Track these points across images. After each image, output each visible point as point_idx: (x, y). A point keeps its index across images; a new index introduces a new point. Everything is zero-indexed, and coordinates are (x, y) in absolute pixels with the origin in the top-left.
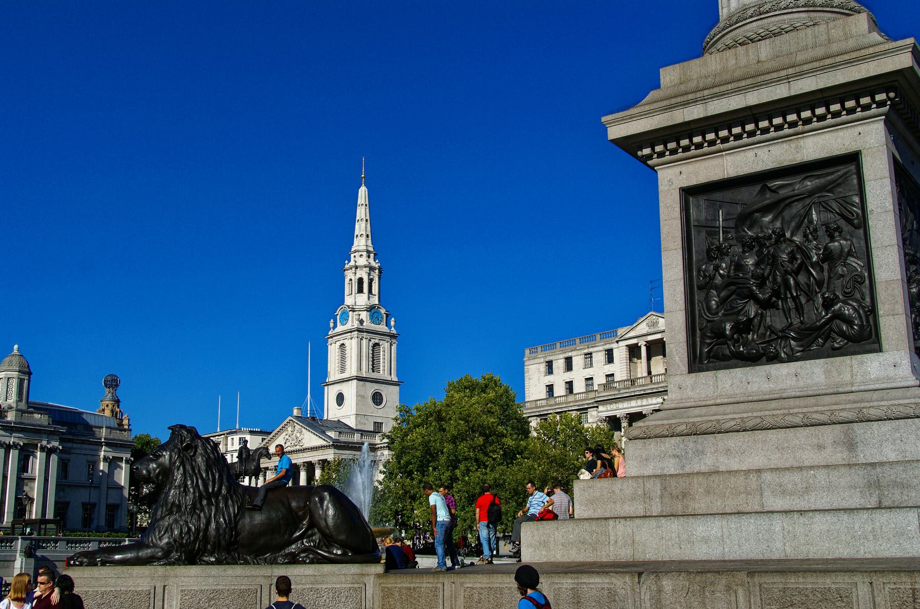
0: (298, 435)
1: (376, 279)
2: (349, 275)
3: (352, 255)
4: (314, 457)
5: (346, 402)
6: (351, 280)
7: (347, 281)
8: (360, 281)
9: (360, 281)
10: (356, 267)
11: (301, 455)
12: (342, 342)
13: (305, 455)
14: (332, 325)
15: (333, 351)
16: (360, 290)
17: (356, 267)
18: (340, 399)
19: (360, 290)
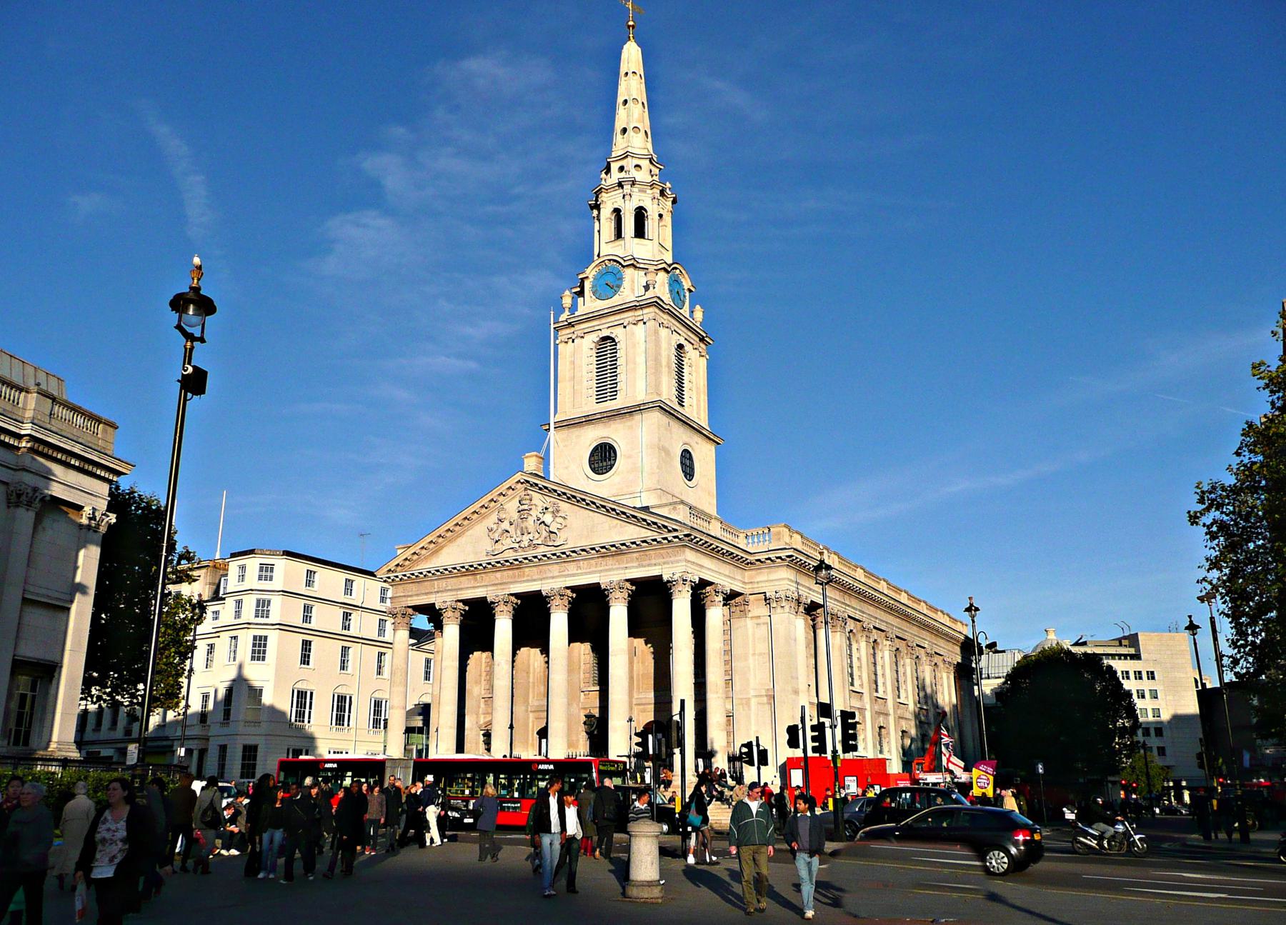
0: (548, 518)
1: (668, 219)
2: (609, 202)
3: (615, 167)
4: (612, 575)
5: (620, 462)
6: (617, 211)
7: (606, 212)
8: (640, 215)
9: (640, 215)
10: (633, 183)
11: (555, 570)
12: (605, 333)
13: (572, 568)
14: (567, 301)
15: (575, 360)
16: (640, 232)
17: (633, 183)
18: (603, 457)
19: (640, 232)
